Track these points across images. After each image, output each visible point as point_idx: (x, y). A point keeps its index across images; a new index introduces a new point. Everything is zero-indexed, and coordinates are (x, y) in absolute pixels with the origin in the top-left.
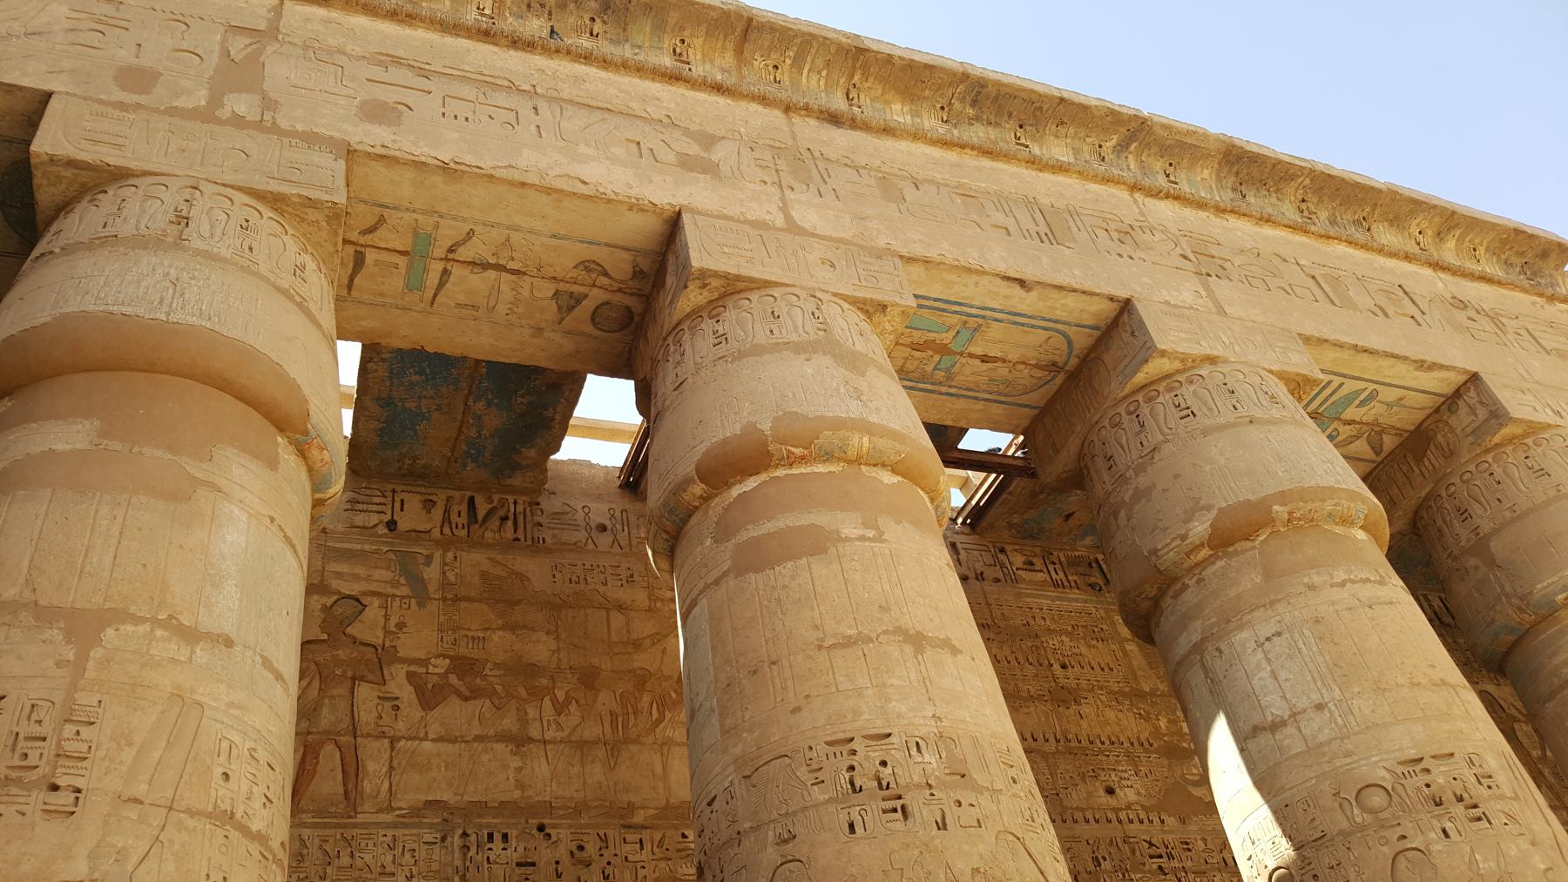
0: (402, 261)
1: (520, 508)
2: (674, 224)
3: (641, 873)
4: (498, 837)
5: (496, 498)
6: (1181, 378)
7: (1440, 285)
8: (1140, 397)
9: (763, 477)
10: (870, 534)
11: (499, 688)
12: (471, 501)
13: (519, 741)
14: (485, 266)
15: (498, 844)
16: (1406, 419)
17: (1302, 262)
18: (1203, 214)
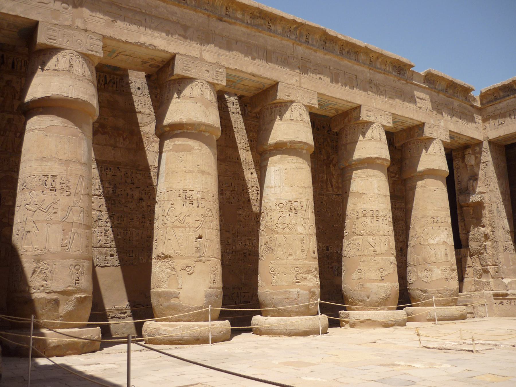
0: (108, 53)
1: (118, 80)
2: (173, 58)
3: (140, 180)
4: (108, 169)
5: (112, 76)
6: (283, 104)
7: (368, 75)
8: (274, 105)
9: (182, 131)
10: (200, 148)
11: (110, 133)
12: (106, 76)
13: (115, 147)
14: (127, 55)
15: (108, 171)
16: (345, 110)
17: (332, 68)
18: (311, 51)
